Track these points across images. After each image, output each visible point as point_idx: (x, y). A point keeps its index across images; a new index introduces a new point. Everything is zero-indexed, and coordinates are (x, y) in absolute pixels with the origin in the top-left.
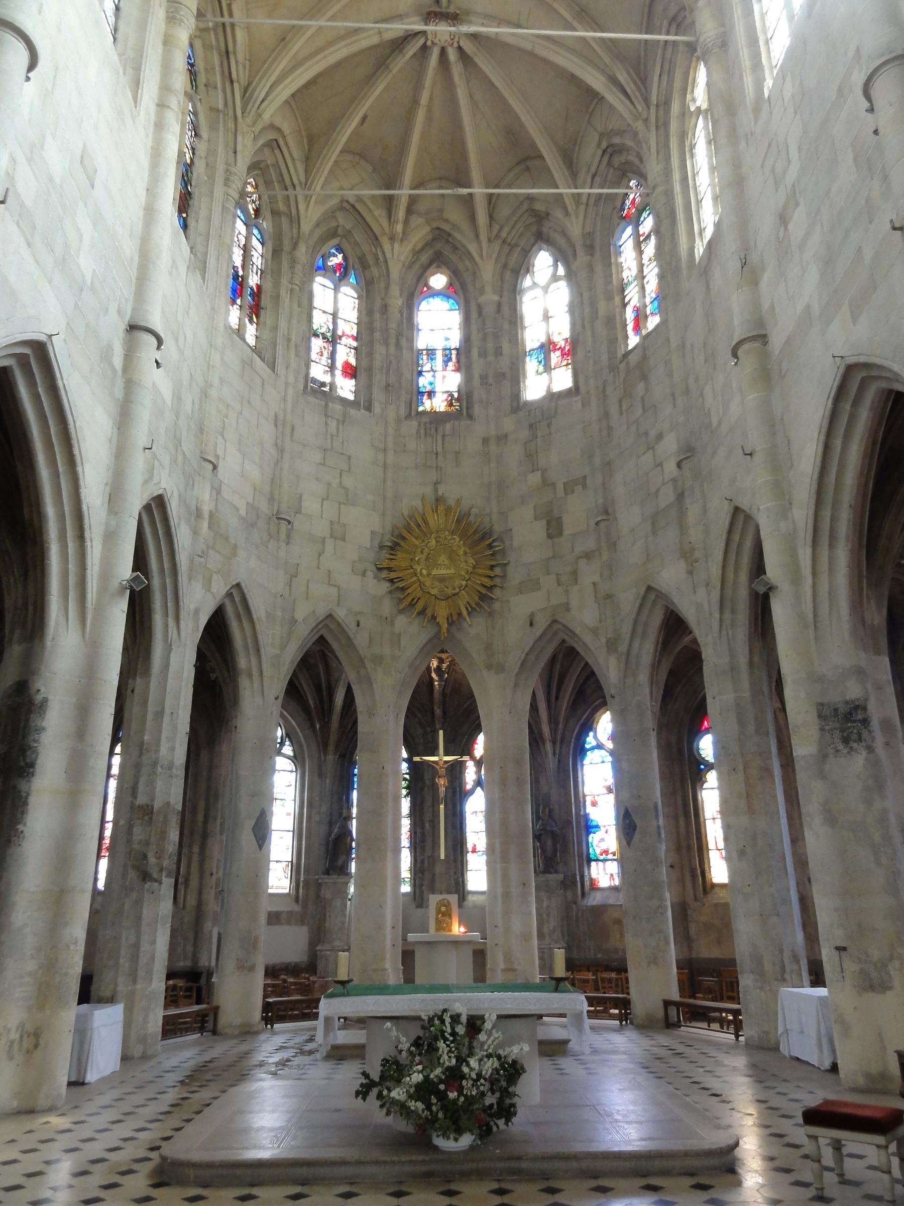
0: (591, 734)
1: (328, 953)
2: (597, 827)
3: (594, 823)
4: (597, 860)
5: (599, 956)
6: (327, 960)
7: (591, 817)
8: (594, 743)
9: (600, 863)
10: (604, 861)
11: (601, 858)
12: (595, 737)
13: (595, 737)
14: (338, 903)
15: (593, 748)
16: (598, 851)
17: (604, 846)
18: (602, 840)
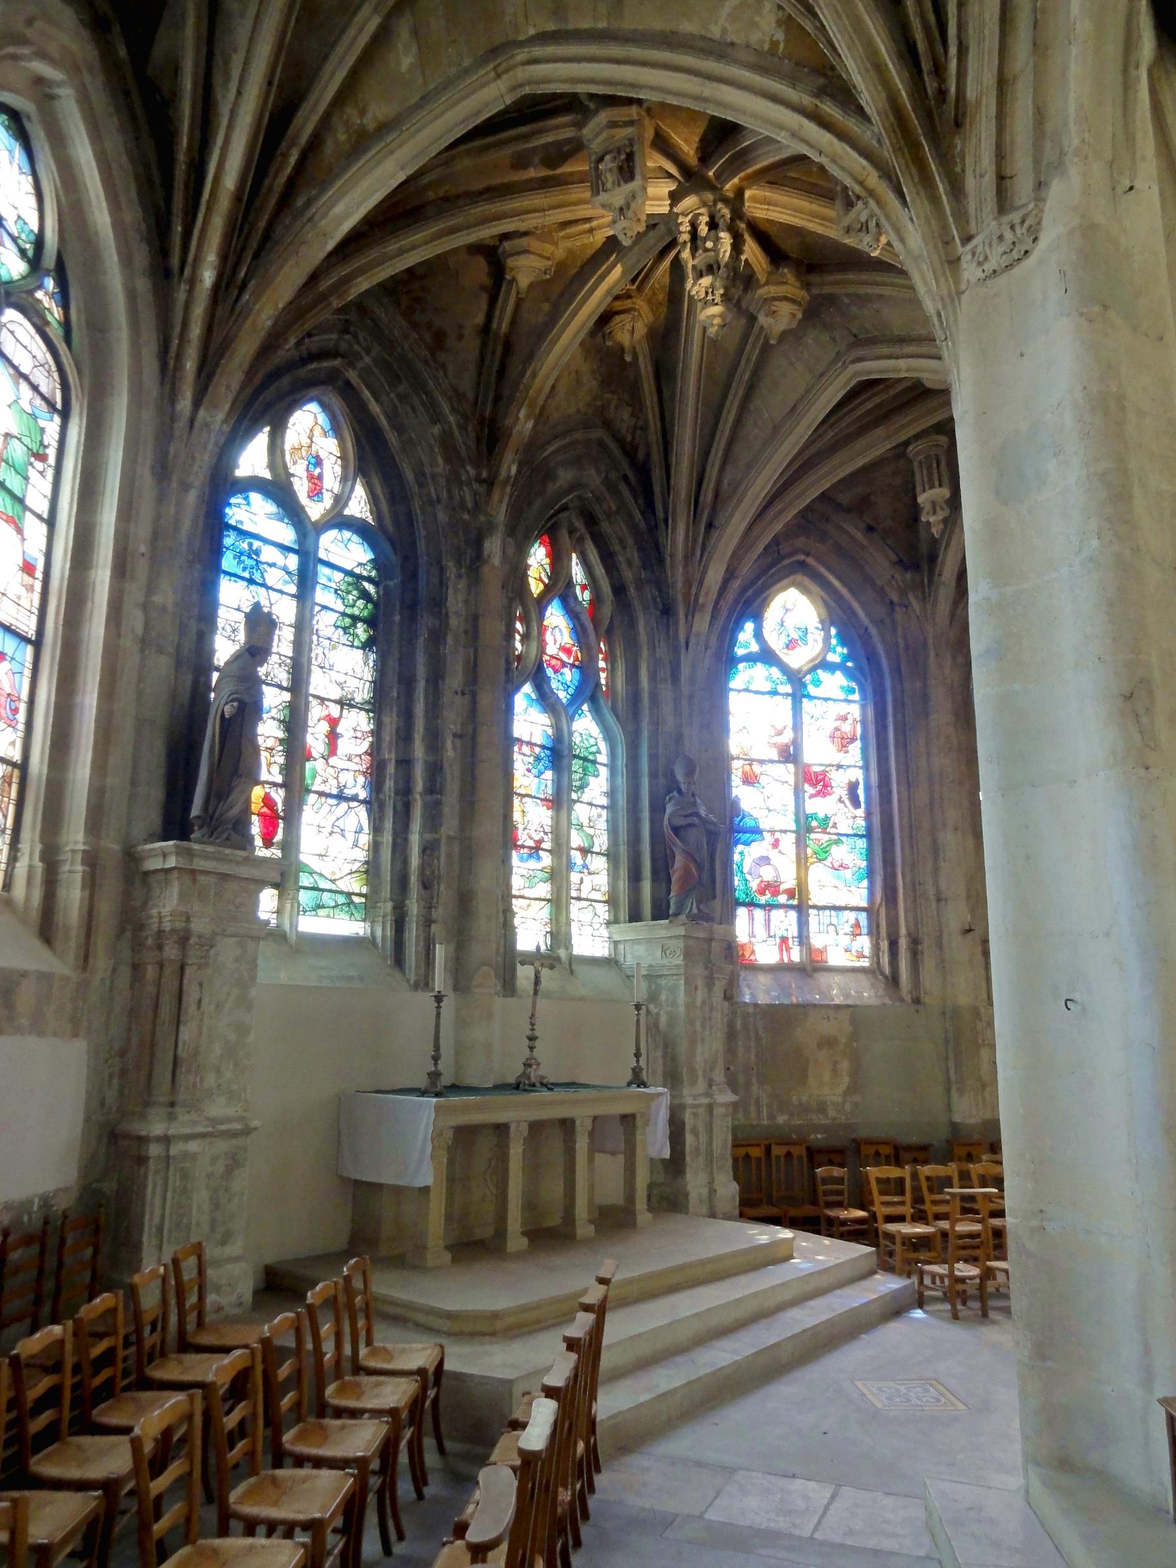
0: (749, 626)
1: (193, 1146)
2: (757, 831)
3: (749, 822)
4: (751, 905)
5: (781, 1119)
6: (185, 1176)
7: (745, 805)
8: (755, 647)
9: (759, 914)
10: (769, 907)
11: (762, 900)
12: (758, 635)
13: (758, 635)
14: (226, 952)
15: (750, 658)
16: (754, 884)
17: (767, 874)
18: (765, 860)
